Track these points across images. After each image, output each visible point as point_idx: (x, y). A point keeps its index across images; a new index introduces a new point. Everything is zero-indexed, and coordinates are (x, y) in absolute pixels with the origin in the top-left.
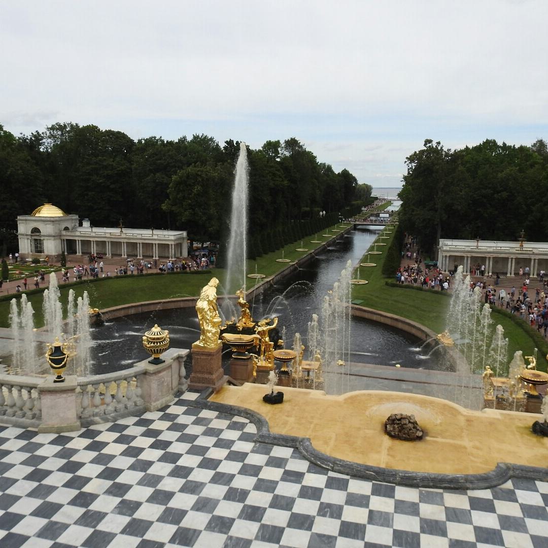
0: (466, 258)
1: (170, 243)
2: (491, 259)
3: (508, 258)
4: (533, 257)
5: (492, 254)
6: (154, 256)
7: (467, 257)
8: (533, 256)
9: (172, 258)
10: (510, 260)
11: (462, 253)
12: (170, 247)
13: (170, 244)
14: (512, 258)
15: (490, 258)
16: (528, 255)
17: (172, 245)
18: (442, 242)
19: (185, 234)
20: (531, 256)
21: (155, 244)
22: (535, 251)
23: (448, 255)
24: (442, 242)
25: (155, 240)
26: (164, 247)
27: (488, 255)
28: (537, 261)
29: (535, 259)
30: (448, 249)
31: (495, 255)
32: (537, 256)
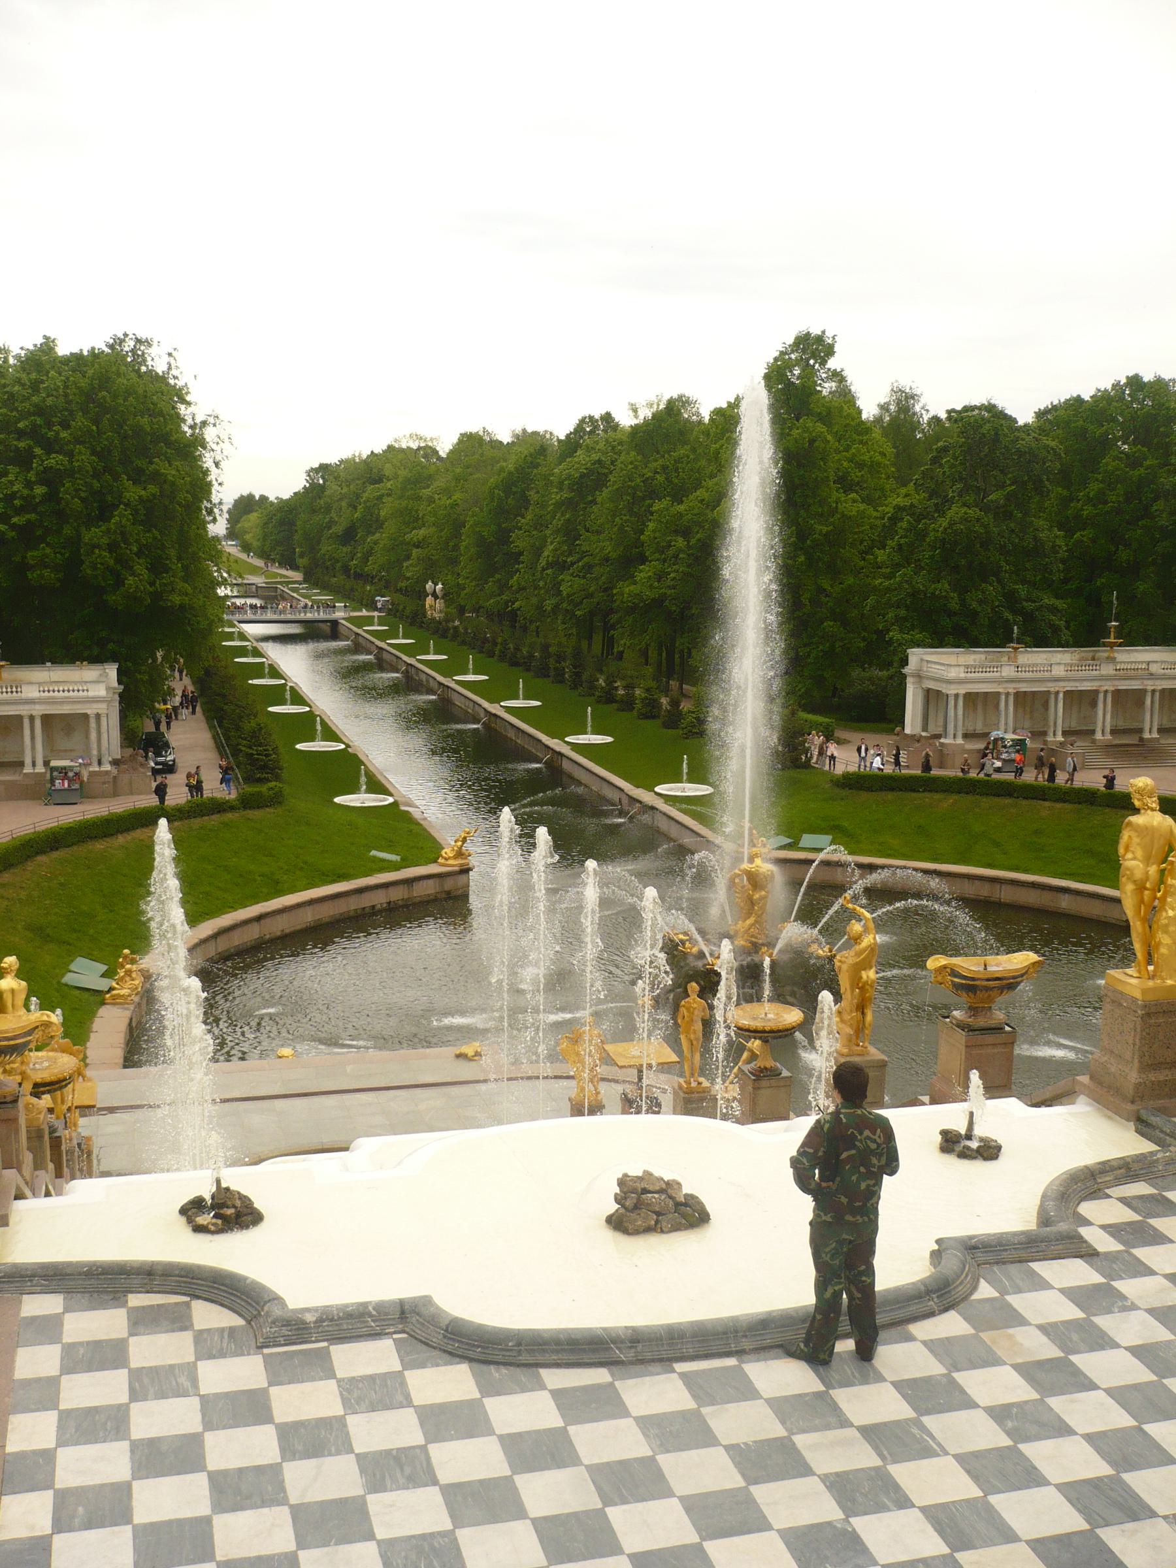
0: (1003, 697)
1: (91, 710)
2: (1061, 695)
3: (1096, 692)
4: (1150, 685)
5: (1062, 684)
6: (28, 761)
7: (1007, 694)
8: (1150, 682)
9: (100, 763)
10: (1101, 696)
11: (995, 685)
12: (93, 724)
13: (89, 712)
14: (1106, 692)
15: (1057, 693)
16: (1138, 682)
17: (98, 716)
18: (917, 657)
19: (112, 671)
20: (1146, 682)
21: (32, 718)
22: (1154, 668)
23: (962, 692)
24: (917, 657)
25: (31, 702)
26: (62, 726)
27: (1052, 687)
28: (1157, 694)
29: (1153, 691)
30: (963, 675)
31: (1070, 686)
32: (1158, 682)
